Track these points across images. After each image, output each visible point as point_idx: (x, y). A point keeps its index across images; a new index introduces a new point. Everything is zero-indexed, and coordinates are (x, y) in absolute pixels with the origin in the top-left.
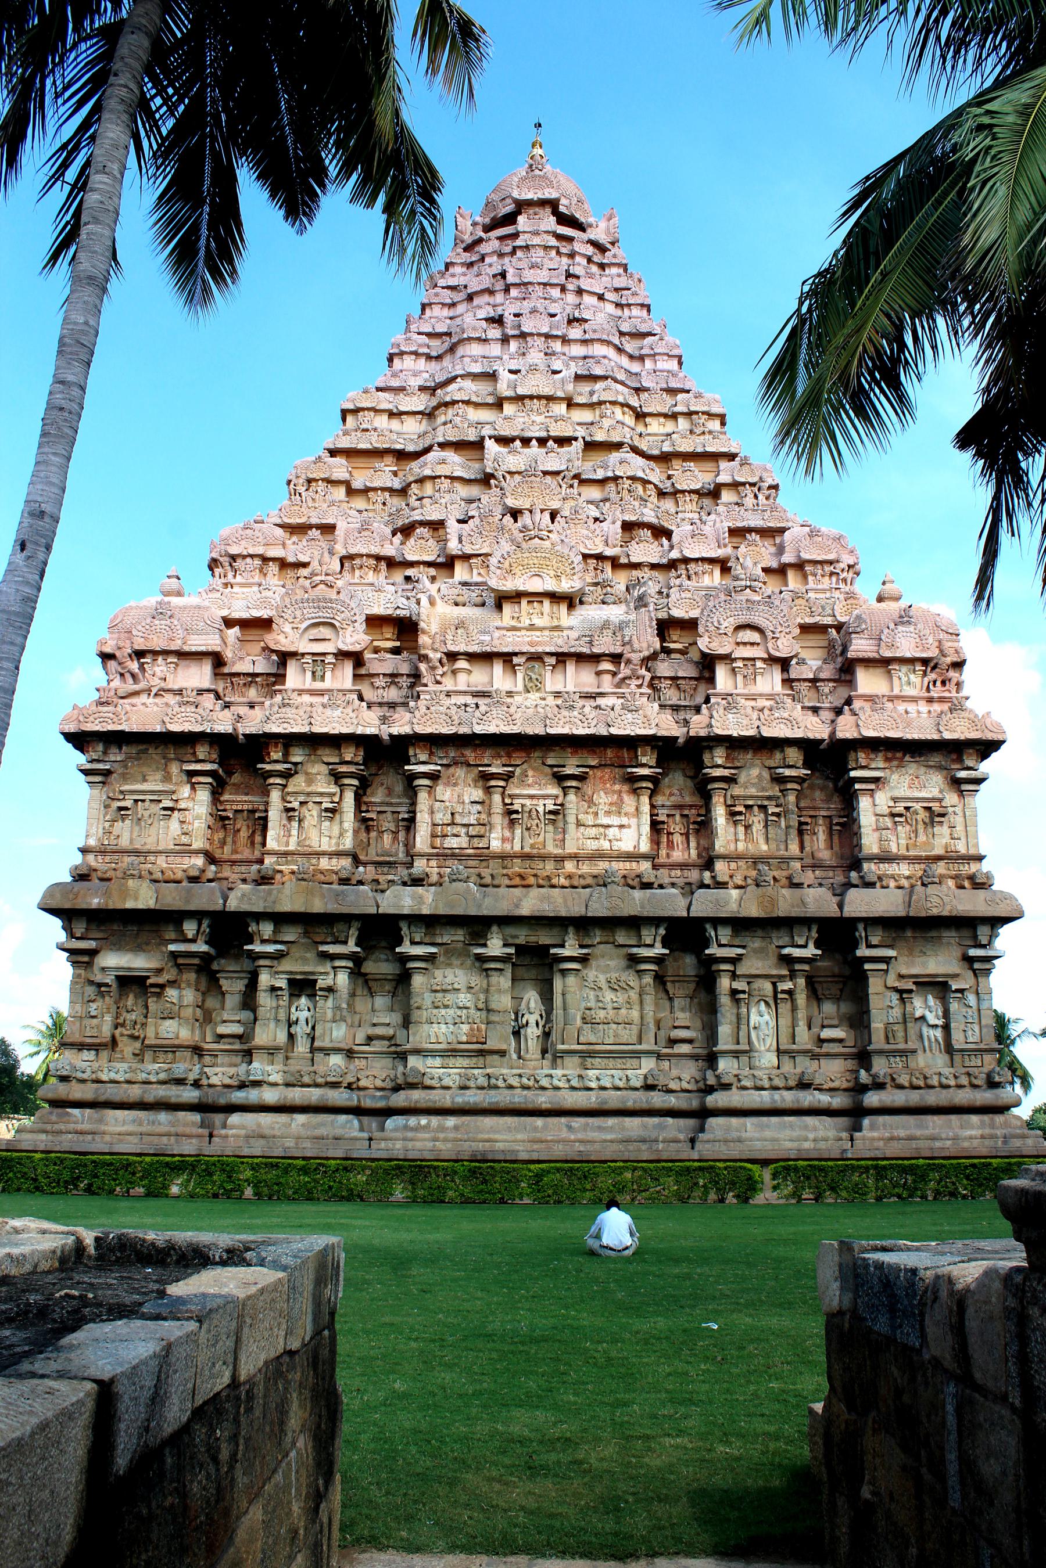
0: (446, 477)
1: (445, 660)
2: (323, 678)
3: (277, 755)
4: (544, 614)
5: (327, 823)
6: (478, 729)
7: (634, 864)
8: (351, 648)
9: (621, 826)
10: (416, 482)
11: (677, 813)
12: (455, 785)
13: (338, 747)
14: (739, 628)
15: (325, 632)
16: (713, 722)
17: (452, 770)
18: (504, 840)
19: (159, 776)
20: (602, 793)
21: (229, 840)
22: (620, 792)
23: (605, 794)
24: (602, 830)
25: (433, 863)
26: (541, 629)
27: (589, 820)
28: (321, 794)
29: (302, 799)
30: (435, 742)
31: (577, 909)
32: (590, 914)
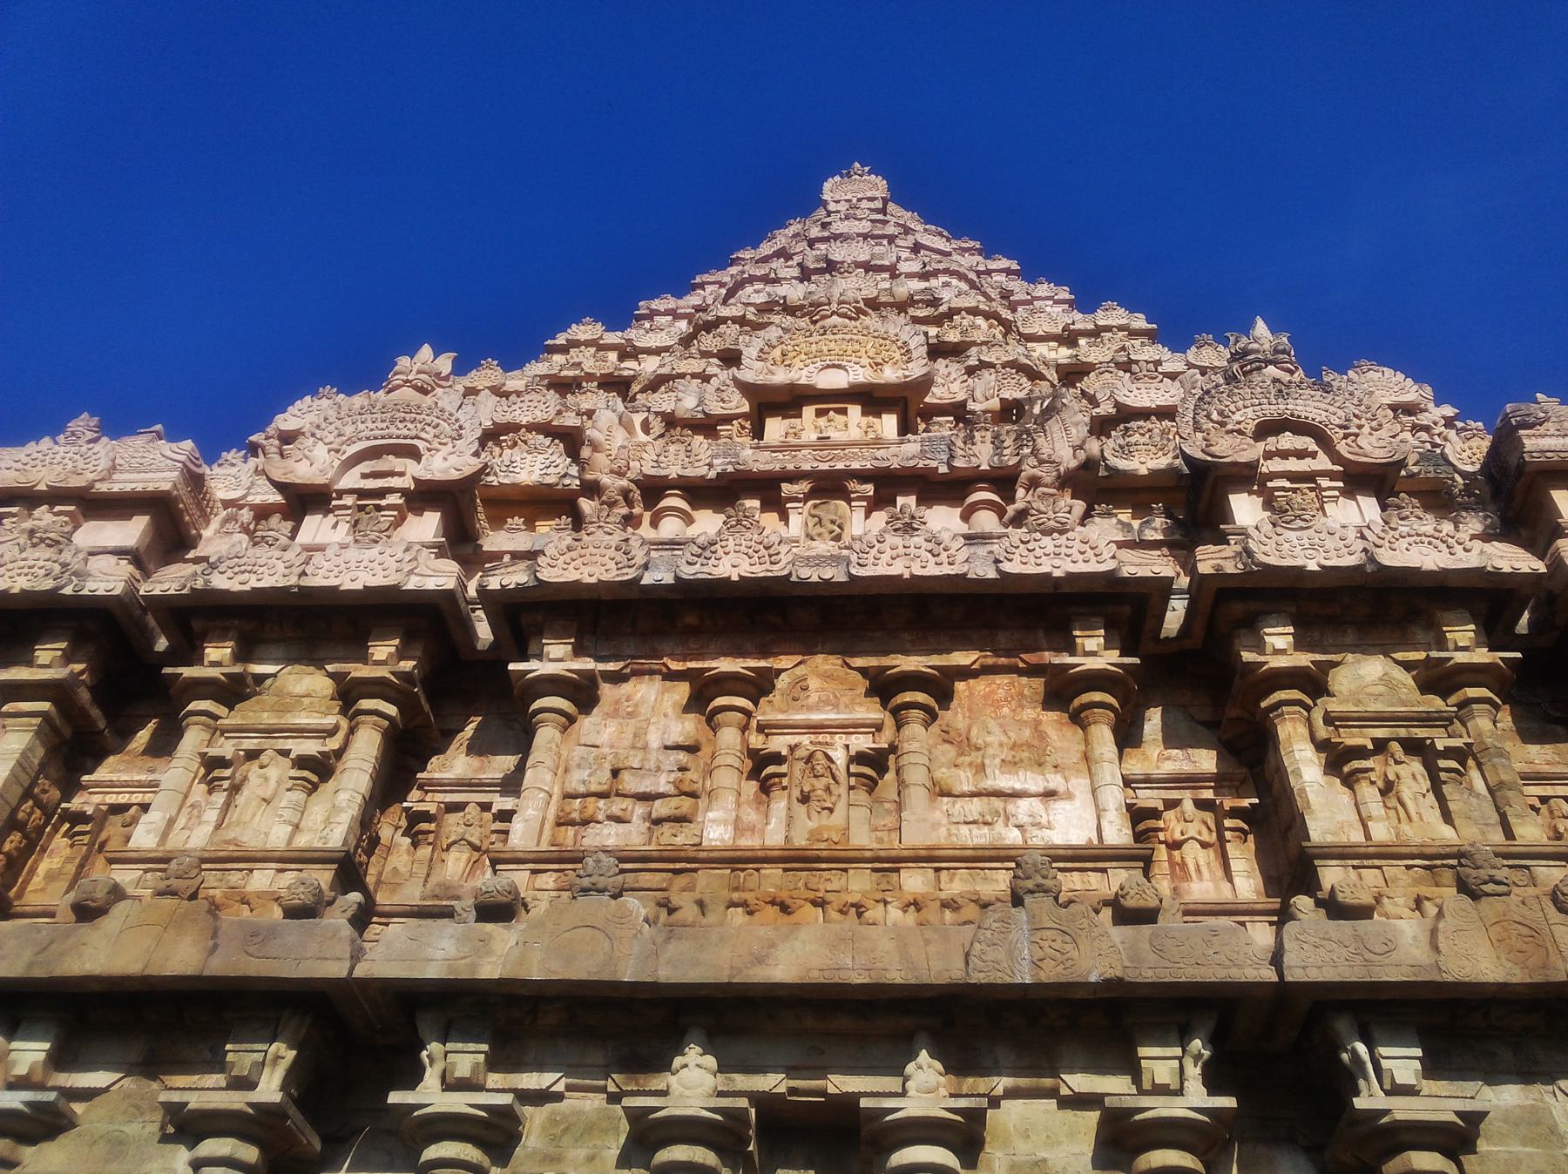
0: (694, 376)
1: (637, 495)
6: (688, 572)
7: (1093, 877)
8: (439, 476)
9: (1049, 795)
11: (1187, 797)
12: (630, 715)
15: (396, 463)
16: (1252, 545)
17: (626, 688)
18: (739, 827)
23: (998, 700)
24: (997, 803)
25: (548, 880)
27: (964, 780)
28: (301, 732)
31: (936, 965)
32: (978, 978)
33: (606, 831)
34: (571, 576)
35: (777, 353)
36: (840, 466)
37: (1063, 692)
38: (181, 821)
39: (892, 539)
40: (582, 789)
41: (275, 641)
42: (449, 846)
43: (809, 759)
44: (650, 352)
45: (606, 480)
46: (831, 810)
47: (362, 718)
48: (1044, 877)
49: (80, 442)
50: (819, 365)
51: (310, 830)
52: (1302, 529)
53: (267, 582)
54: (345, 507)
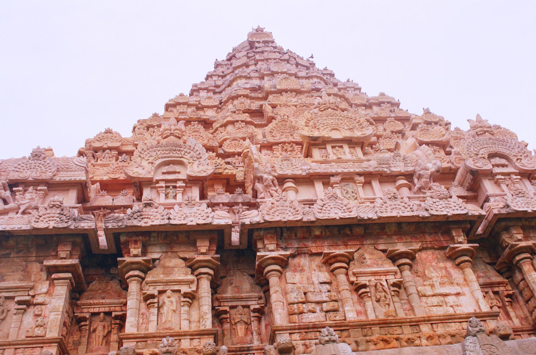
1: (276, 182)
2: (175, 197)
3: (135, 250)
4: (346, 152)
5: (186, 308)
9: (458, 294)
10: (221, 126)
12: (302, 270)
13: (193, 244)
14: (491, 156)
17: (296, 260)
18: (358, 313)
19: (19, 275)
20: (431, 269)
21: (84, 340)
22: (446, 268)
24: (442, 298)
25: (296, 336)
26: (347, 161)
27: (429, 291)
28: (180, 282)
29: (160, 288)
30: (282, 231)
33: (310, 316)
34: (277, 219)
35: (311, 123)
36: (352, 170)
37: (453, 256)
38: (141, 321)
39: (389, 202)
40: (296, 301)
41: (154, 245)
42: (236, 323)
43: (376, 286)
44: (208, 107)
45: (265, 176)
46: (389, 305)
47: (203, 276)
48: (481, 326)
49: (40, 158)
50: (329, 128)
51: (194, 322)
52: (522, 197)
53: (157, 222)
54: (162, 187)
